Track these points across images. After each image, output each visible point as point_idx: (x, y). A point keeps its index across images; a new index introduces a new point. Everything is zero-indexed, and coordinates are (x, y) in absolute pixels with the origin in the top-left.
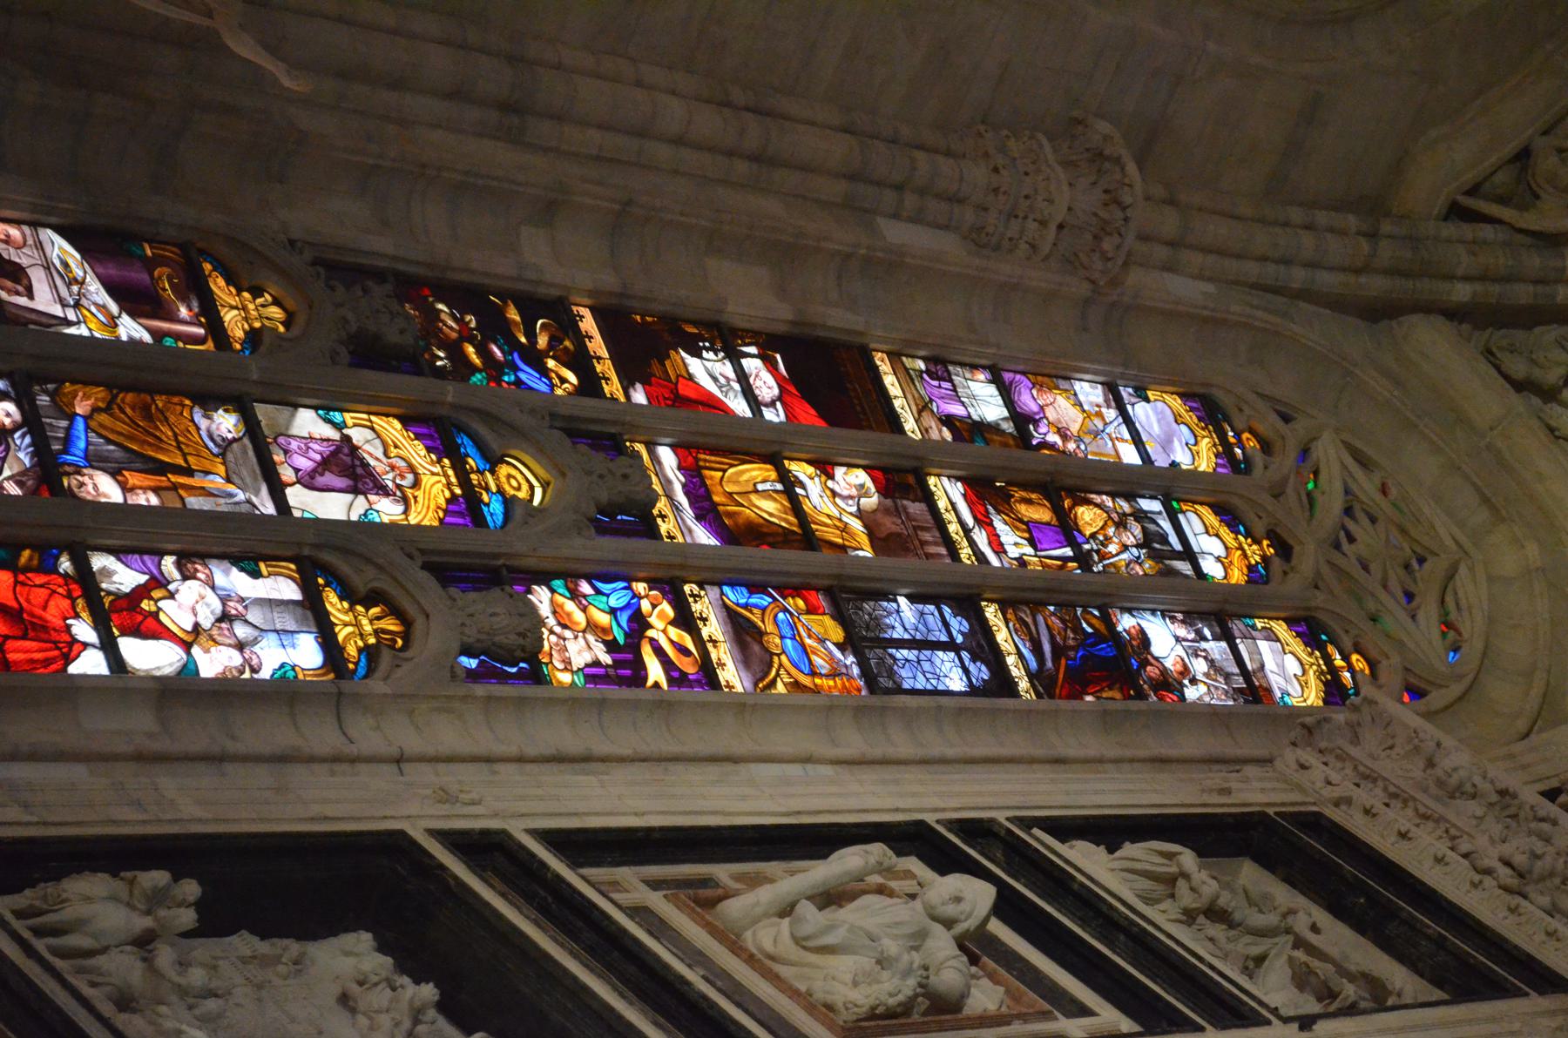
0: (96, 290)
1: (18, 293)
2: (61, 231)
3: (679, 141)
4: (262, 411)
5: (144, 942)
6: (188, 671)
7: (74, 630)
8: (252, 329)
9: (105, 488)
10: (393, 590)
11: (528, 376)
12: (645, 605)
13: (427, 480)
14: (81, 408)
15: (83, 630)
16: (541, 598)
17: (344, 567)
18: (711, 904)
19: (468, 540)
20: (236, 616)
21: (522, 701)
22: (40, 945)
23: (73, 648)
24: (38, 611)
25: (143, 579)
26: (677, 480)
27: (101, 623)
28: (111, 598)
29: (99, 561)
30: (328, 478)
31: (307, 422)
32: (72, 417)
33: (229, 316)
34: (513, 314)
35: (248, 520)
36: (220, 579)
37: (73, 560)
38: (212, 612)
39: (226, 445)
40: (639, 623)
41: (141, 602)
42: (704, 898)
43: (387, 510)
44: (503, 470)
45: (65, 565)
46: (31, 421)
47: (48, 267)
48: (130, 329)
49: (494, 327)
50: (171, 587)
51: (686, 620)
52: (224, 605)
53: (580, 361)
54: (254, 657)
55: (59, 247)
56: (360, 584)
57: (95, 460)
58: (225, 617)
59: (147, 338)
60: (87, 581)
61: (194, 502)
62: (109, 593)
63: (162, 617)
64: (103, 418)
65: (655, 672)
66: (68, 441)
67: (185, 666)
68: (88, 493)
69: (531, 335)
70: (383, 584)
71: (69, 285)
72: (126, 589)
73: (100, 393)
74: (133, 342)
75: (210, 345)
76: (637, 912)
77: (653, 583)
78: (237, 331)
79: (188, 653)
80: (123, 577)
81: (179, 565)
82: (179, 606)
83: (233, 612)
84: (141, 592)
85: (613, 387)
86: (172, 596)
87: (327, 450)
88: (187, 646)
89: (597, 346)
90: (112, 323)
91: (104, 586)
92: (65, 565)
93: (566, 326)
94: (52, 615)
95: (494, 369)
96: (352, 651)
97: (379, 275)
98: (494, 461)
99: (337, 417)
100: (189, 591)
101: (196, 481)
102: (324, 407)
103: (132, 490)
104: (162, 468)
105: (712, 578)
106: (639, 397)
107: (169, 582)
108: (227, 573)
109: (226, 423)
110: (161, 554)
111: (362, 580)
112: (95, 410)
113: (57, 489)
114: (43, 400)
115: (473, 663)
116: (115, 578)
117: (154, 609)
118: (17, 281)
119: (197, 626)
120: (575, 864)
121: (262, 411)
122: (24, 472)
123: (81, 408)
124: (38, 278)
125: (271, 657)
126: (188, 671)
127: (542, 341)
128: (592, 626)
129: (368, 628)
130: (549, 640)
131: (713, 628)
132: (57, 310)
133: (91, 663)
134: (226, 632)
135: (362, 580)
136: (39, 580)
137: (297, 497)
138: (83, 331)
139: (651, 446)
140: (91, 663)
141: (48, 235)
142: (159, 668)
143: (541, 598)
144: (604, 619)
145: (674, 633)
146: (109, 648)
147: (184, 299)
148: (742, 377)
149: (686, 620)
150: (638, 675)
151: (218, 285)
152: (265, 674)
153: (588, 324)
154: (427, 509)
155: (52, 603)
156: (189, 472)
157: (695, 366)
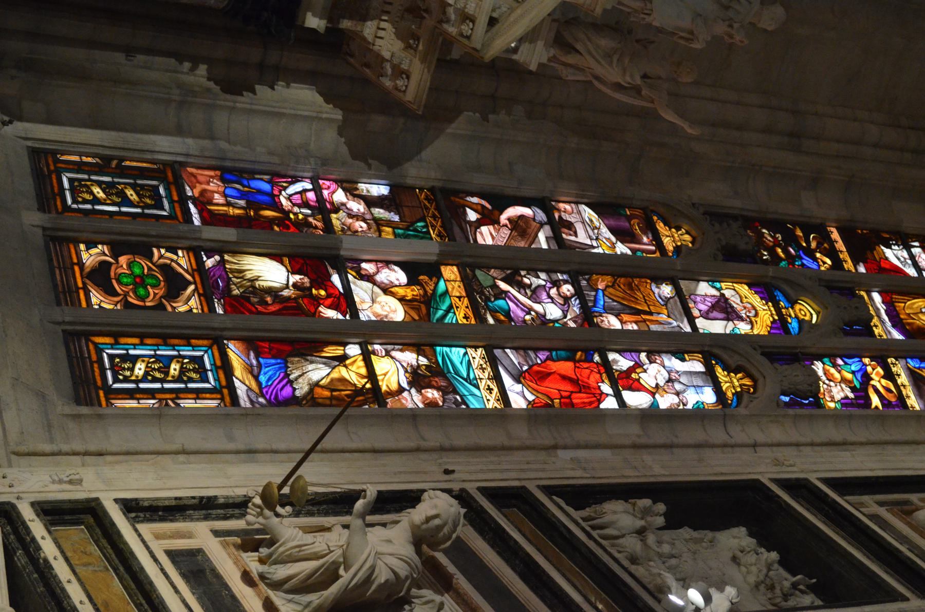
0: (605, 232)
1: (571, 235)
2: (587, 205)
3: (876, 146)
4: (683, 284)
5: (641, 532)
6: (654, 406)
7: (602, 388)
8: (677, 246)
9: (613, 322)
10: (748, 366)
11: (807, 261)
12: (869, 369)
13: (761, 313)
14: (601, 286)
15: (606, 388)
16: (818, 367)
17: (725, 356)
18: (910, 513)
19: (782, 341)
20: (675, 380)
21: (811, 417)
22: (595, 534)
23: (601, 396)
24: (586, 380)
25: (632, 363)
26: (882, 308)
27: (614, 384)
28: (618, 373)
29: (612, 356)
30: (715, 314)
31: (704, 288)
32: (597, 290)
33: (666, 241)
34: (799, 233)
35: (678, 335)
36: (667, 363)
37: (600, 356)
38: (664, 378)
39: (667, 300)
40: (866, 378)
41: (631, 374)
42: (906, 511)
43: (743, 328)
44: (797, 307)
45: (597, 358)
46: (579, 293)
47: (583, 222)
48: (622, 248)
49: (791, 239)
50: (645, 367)
51: (889, 375)
52: (669, 374)
53: (832, 253)
54: (684, 398)
55: (588, 213)
56: (732, 363)
57: (608, 310)
58: (670, 380)
59: (629, 252)
60: (607, 365)
61: (654, 327)
62: (617, 371)
63: (641, 381)
64: (611, 290)
65: (876, 401)
66: (595, 301)
67: (652, 403)
68: (605, 325)
69: (808, 242)
70: (742, 362)
71: (593, 230)
72: (625, 368)
73: (609, 278)
74: (623, 255)
75: (658, 254)
76: (872, 517)
77: (872, 359)
78: (670, 248)
79: (654, 397)
80: (623, 363)
81: (648, 357)
82: (649, 376)
83: (674, 378)
84: (631, 370)
85: (849, 265)
86: (645, 371)
87: (714, 300)
88: (653, 394)
89: (840, 245)
90: (613, 246)
91: (614, 367)
92: (597, 358)
93: (825, 237)
94: (592, 382)
95: (791, 259)
96: (729, 394)
97: (735, 218)
98: (792, 303)
99: (718, 285)
100: (653, 368)
101: (654, 318)
102: (712, 281)
103: (625, 323)
104: (638, 312)
105: (901, 353)
106: (862, 269)
107: (644, 365)
108: (670, 360)
109: (667, 290)
110: (640, 352)
111: (733, 362)
112: (607, 286)
113: (591, 324)
114: (584, 283)
115: (787, 399)
116: (619, 364)
117: (637, 377)
118: (570, 229)
119: (657, 385)
120: (842, 494)
121: (683, 284)
122: (576, 317)
123: (601, 286)
124: (579, 227)
125: (692, 399)
126: (654, 406)
127: (814, 245)
128: (844, 380)
129: (737, 384)
130: (823, 387)
131: (903, 379)
132: (588, 242)
133: (610, 403)
134: (671, 387)
135: (733, 362)
136: (586, 365)
137: (701, 323)
138: (600, 250)
139: (869, 293)
140: (610, 403)
141: (583, 208)
142: (641, 405)
143: (818, 367)
144: (849, 376)
145: (884, 382)
146: (618, 396)
147: (645, 234)
148: (912, 257)
149: (889, 375)
150: (868, 401)
151: (660, 226)
152: (690, 406)
153: (835, 235)
154: (761, 328)
155: (592, 376)
156: (651, 313)
157: (888, 253)
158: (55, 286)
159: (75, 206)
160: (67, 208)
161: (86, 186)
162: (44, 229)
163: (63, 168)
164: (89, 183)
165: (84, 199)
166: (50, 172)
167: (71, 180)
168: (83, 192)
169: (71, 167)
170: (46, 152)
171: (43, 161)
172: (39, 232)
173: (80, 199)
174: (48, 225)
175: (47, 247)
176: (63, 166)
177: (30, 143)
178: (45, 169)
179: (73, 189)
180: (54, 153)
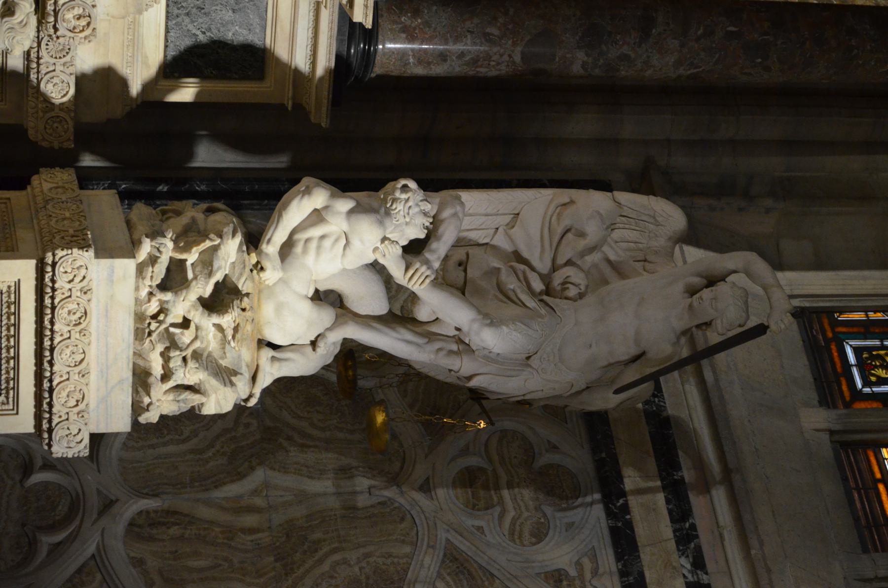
158: (856, 519)
159: (867, 390)
160: (857, 395)
161: (879, 357)
162: (832, 432)
163: (844, 333)
164: (882, 352)
165: (878, 377)
166: (828, 341)
167: (857, 351)
168: (876, 367)
169: (855, 330)
170: (818, 311)
171: (816, 326)
172: (826, 437)
173: (873, 379)
174: (837, 427)
175: (837, 458)
176: (844, 330)
177: (796, 303)
178: (821, 337)
179: (861, 365)
180: (830, 312)
